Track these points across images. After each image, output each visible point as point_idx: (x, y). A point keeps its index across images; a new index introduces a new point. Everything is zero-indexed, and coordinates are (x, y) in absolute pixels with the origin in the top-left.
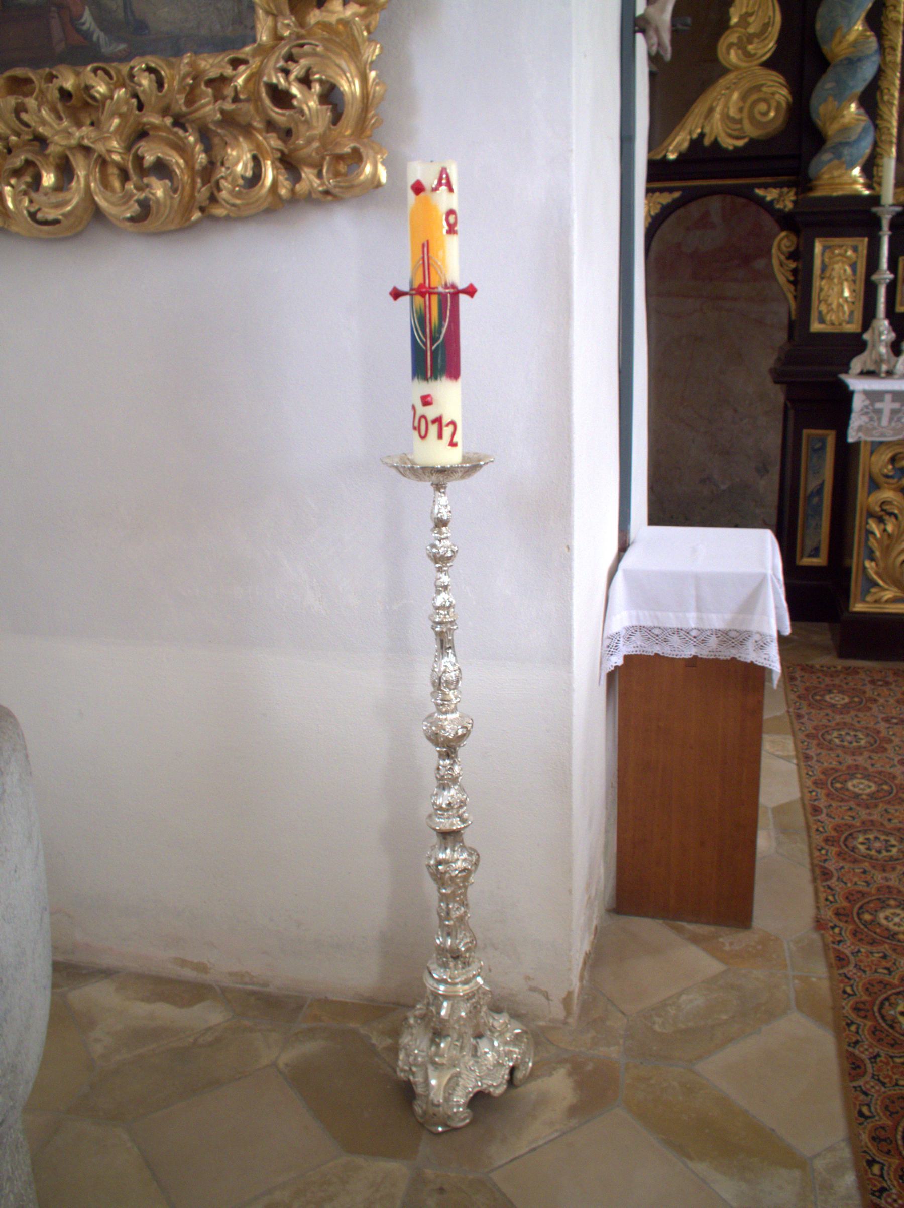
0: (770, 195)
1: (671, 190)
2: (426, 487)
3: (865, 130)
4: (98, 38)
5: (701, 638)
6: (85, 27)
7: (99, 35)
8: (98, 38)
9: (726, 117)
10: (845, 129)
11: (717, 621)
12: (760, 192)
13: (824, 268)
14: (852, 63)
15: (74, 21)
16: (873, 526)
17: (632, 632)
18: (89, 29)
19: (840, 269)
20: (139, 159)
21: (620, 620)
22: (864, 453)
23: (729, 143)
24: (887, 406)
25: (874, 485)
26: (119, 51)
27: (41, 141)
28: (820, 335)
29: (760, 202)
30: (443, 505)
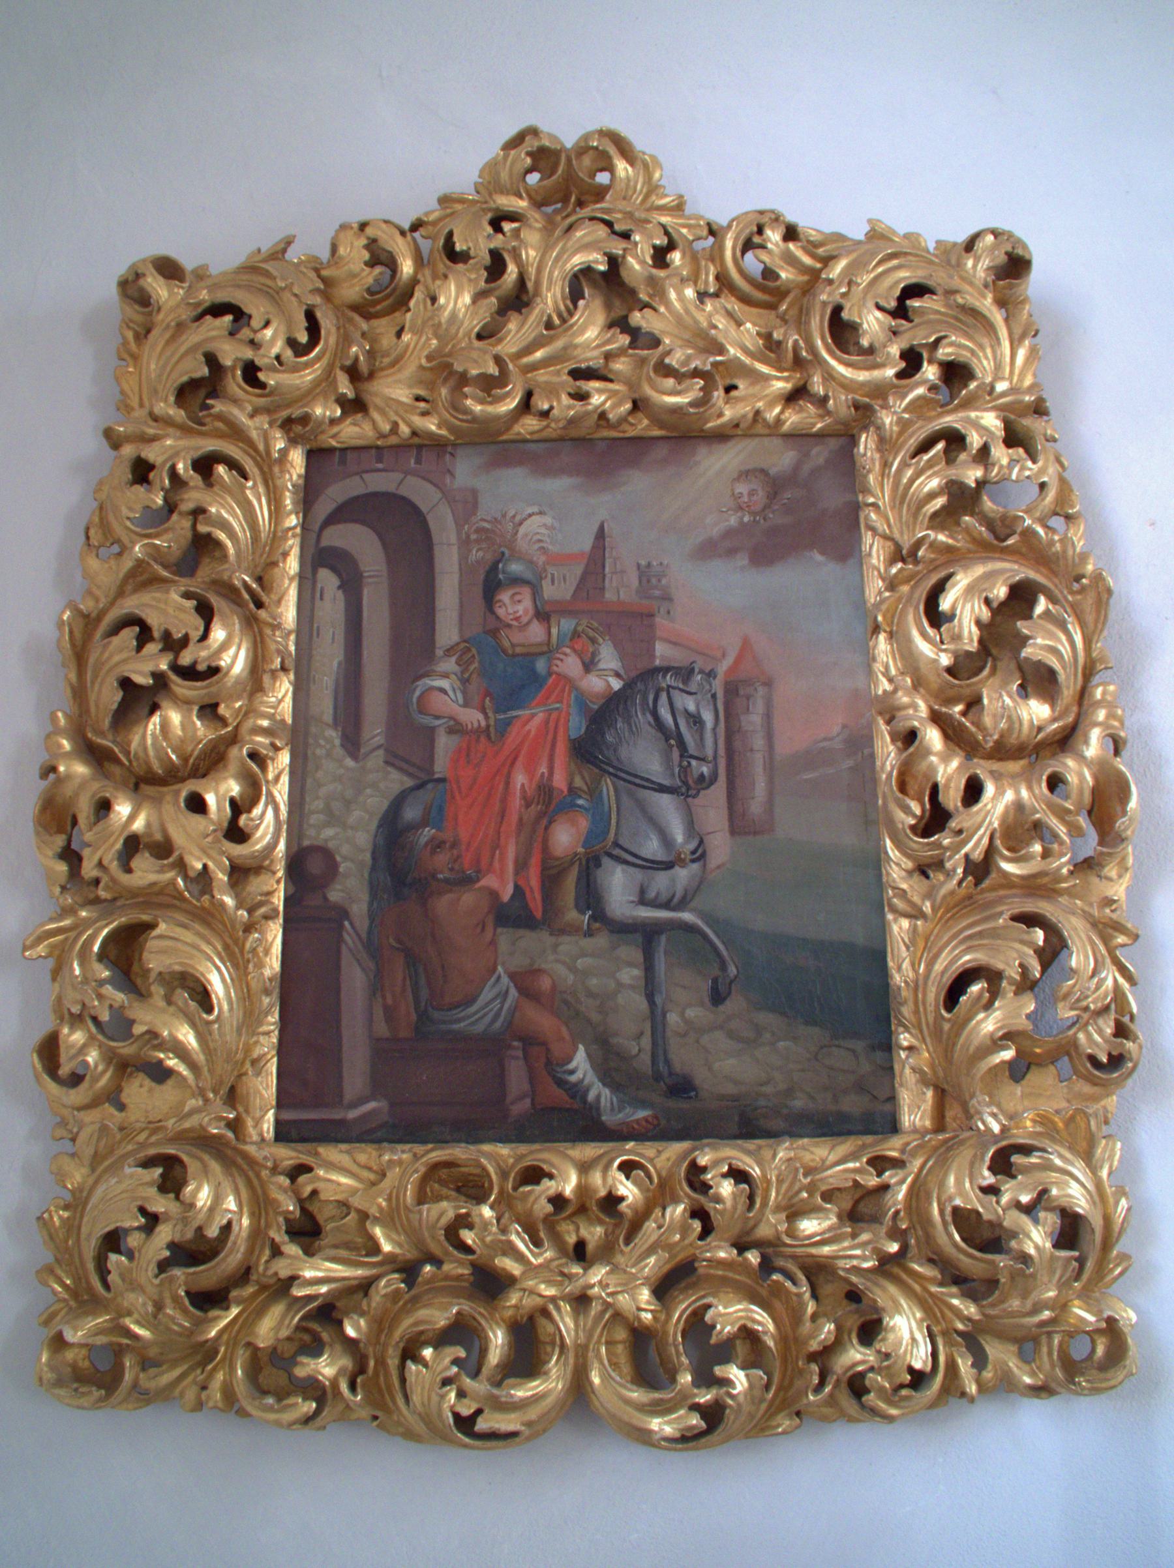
4: (598, 1097)
6: (573, 1078)
7: (599, 1093)
8: (598, 1097)
18: (582, 1081)
20: (698, 1326)
26: (637, 1121)
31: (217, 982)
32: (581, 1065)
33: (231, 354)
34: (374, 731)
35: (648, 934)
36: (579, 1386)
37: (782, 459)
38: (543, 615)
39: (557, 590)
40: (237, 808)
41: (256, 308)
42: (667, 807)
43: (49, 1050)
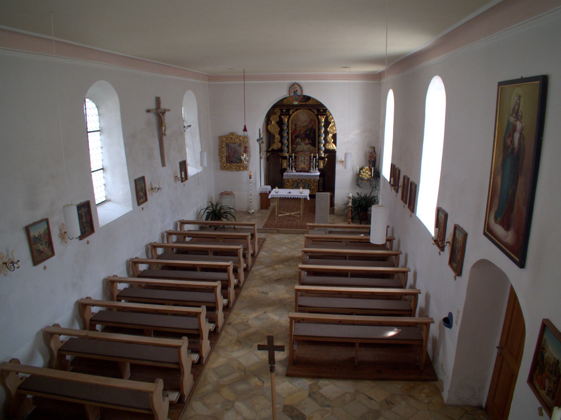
0: (280, 154)
5: (265, 191)
10: (285, 150)
11: (265, 190)
16: (286, 186)
17: (261, 191)
21: (260, 190)
22: (285, 180)
23: (276, 149)
24: (286, 176)
25: (286, 182)
27: (231, 167)
28: (283, 168)
31: (224, 159)
32: (234, 161)
35: (235, 158)
43: (220, 161)
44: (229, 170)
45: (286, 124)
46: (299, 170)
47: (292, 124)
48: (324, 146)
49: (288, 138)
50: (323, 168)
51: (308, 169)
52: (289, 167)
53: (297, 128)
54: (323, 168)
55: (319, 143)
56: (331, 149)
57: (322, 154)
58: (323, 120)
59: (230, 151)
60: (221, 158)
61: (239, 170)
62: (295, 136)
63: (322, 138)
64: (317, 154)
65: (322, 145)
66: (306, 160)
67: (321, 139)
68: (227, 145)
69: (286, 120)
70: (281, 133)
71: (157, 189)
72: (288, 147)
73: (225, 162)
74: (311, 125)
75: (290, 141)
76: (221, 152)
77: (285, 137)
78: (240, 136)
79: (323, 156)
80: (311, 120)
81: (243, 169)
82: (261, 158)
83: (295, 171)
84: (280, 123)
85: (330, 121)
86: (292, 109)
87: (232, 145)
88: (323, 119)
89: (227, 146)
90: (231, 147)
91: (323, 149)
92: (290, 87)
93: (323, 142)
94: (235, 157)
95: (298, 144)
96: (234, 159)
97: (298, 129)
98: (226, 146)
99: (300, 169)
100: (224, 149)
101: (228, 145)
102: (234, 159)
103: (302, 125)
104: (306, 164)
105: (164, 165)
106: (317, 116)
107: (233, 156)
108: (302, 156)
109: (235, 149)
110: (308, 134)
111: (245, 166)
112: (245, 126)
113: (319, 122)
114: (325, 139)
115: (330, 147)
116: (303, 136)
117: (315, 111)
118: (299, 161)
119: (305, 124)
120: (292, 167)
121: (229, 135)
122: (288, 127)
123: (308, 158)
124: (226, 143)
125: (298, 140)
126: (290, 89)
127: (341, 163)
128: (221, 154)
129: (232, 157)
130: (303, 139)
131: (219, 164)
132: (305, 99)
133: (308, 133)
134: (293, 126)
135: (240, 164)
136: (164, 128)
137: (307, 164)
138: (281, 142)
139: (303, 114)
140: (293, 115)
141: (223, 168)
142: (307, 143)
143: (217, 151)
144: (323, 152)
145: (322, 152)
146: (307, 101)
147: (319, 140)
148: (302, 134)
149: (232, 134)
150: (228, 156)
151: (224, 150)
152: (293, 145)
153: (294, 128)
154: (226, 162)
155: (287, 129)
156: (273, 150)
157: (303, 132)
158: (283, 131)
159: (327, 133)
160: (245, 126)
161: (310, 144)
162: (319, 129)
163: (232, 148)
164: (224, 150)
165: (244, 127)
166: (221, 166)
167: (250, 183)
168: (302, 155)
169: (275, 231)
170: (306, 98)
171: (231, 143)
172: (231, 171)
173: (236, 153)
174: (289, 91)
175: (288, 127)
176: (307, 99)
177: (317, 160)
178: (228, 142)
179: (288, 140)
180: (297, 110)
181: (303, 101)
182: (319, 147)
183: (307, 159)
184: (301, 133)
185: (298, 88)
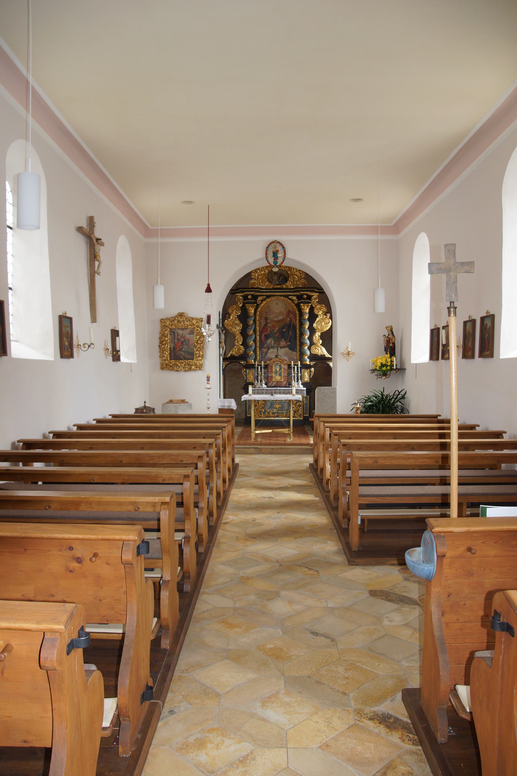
0: (242, 363)
1: (228, 362)
2: (207, 389)
3: (253, 355)
9: (235, 352)
10: (251, 355)
12: (241, 362)
13: (249, 374)
14: (251, 347)
15: (180, 357)
19: (251, 374)
21: (220, 404)
23: (236, 355)
29: (241, 364)
30: (208, 391)
31: (167, 353)
32: (182, 357)
33: (166, 325)
34: (173, 342)
36: (181, 369)
37: (191, 329)
38: (180, 337)
39: (181, 336)
40: (168, 346)
41: (167, 322)
42: (185, 346)
43: (160, 356)
44: (173, 369)
45: (251, 317)
46: (273, 385)
47: (260, 319)
48: (309, 348)
49: (256, 338)
50: (309, 381)
51: (286, 384)
52: (258, 382)
53: (269, 324)
54: (309, 381)
55: (302, 344)
56: (319, 354)
57: (306, 361)
58: (307, 311)
59: (176, 340)
60: (162, 350)
61: (190, 369)
62: (264, 335)
63: (306, 337)
64: (299, 362)
65: (306, 347)
66: (283, 370)
67: (304, 339)
68: (172, 332)
69: (253, 311)
70: (244, 333)
71: (87, 346)
72: (255, 351)
73: (167, 358)
74: (289, 319)
75: (258, 343)
76: (163, 341)
77: (251, 335)
78: (193, 319)
79: (308, 363)
80: (289, 311)
81: (196, 367)
82: (220, 355)
83: (265, 386)
84: (244, 317)
85: (317, 313)
86: (260, 296)
87: (180, 332)
88: (308, 309)
89: (172, 333)
90: (178, 335)
91: (308, 353)
92: (268, 247)
93: (308, 342)
94: (183, 349)
95: (270, 347)
96: (181, 352)
97: (269, 325)
98: (170, 334)
99: (274, 384)
100: (167, 337)
101: (174, 333)
102: (181, 352)
103: (276, 319)
104: (283, 374)
105: (94, 319)
106: (298, 306)
107: (181, 350)
108: (277, 364)
109: (184, 337)
110: (284, 332)
111: (198, 364)
112: (209, 285)
113: (301, 314)
114: (310, 338)
115: (317, 351)
116: (277, 335)
117: (294, 298)
118: (272, 372)
119: (280, 318)
120: (261, 381)
121: (176, 316)
122: (255, 321)
123: (286, 367)
124: (170, 329)
125: (270, 341)
126: (267, 250)
127: (344, 357)
128: (163, 345)
129: (179, 351)
130: (277, 340)
131: (157, 361)
132: (280, 280)
133: (284, 330)
134: (262, 321)
135: (191, 361)
136: (97, 263)
137: (284, 376)
138: (245, 344)
139: (277, 304)
140: (263, 305)
141: (164, 367)
142: (283, 346)
143: (157, 342)
144: (308, 358)
145: (306, 357)
146: (284, 284)
147: (302, 340)
148: (276, 333)
149: (181, 315)
150: (172, 349)
151: (168, 339)
152: (263, 349)
153: (263, 323)
154: (169, 357)
155: (254, 325)
156: (233, 357)
157: (277, 329)
158: (247, 328)
159: (312, 331)
160: (209, 285)
161: (288, 346)
162: (301, 324)
163: (179, 337)
164: (168, 340)
165: (207, 286)
166: (162, 365)
167: (208, 389)
168: (277, 362)
169: (253, 450)
170: (282, 280)
171: (179, 329)
172: (177, 371)
173: (184, 344)
174: (266, 252)
175: (255, 321)
176: (283, 280)
177: (299, 369)
178: (173, 327)
179: (255, 341)
180: (268, 297)
181: (277, 283)
182: (302, 350)
183: (284, 369)
184: (274, 331)
185: (280, 248)
